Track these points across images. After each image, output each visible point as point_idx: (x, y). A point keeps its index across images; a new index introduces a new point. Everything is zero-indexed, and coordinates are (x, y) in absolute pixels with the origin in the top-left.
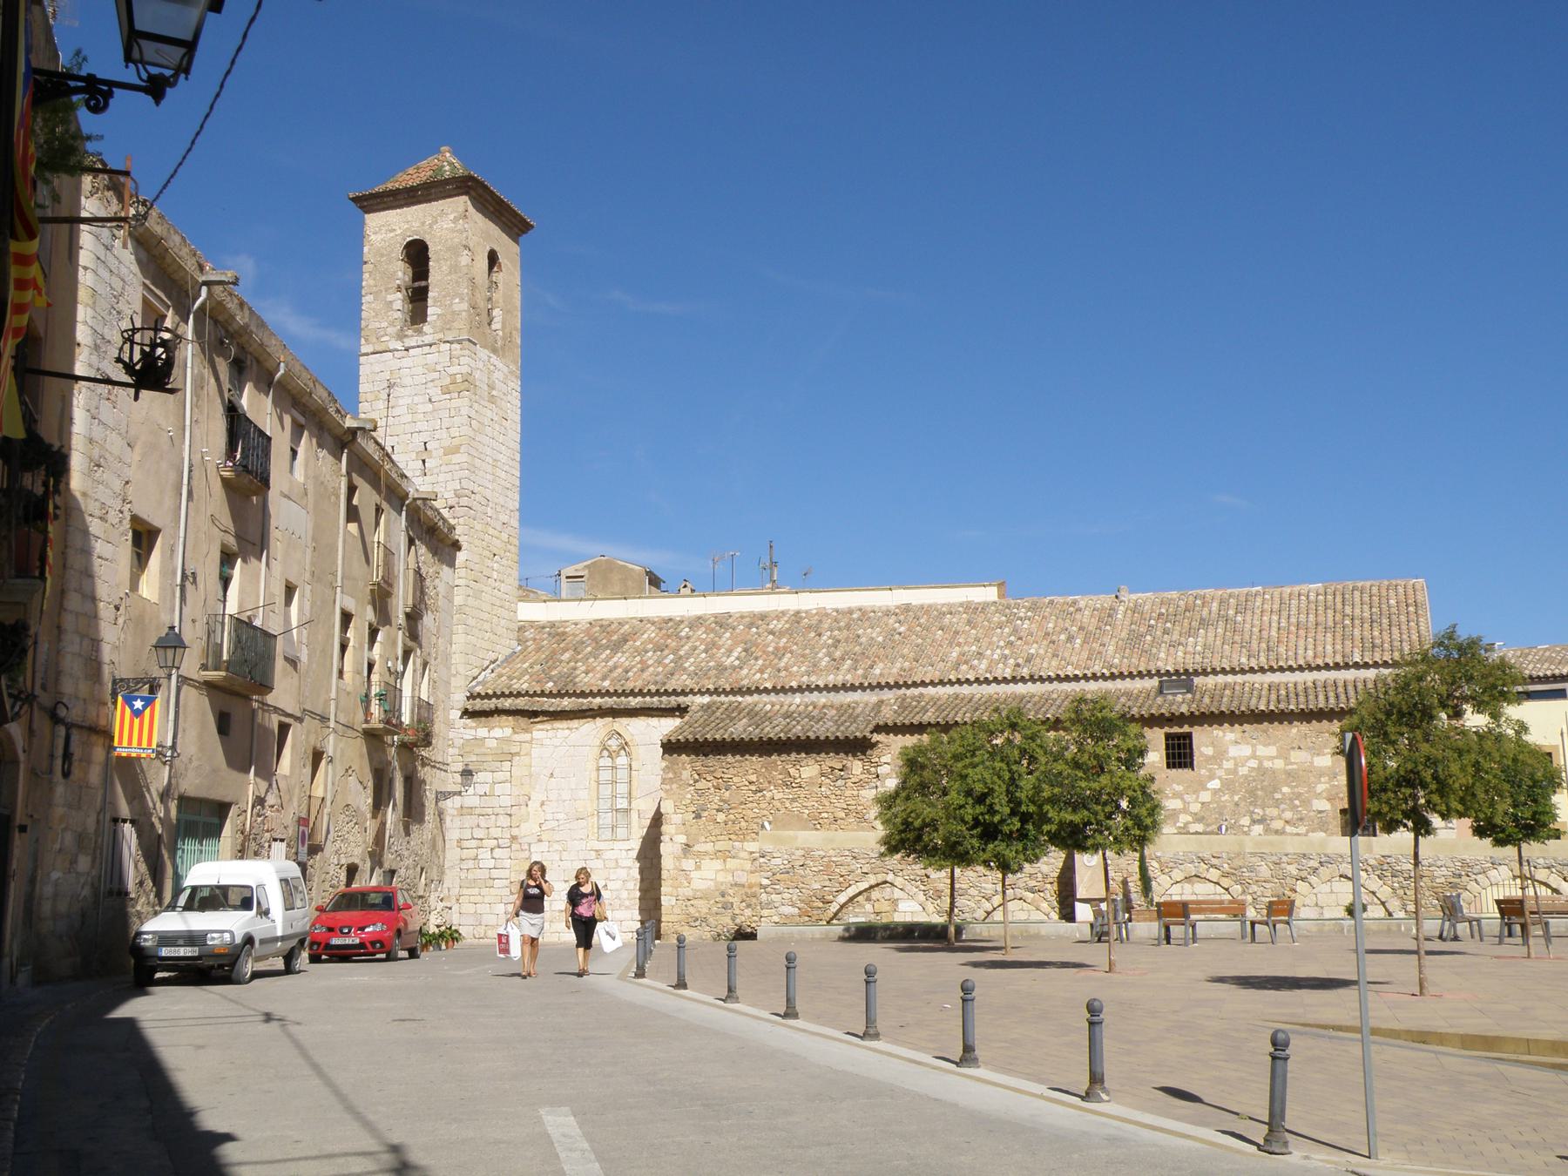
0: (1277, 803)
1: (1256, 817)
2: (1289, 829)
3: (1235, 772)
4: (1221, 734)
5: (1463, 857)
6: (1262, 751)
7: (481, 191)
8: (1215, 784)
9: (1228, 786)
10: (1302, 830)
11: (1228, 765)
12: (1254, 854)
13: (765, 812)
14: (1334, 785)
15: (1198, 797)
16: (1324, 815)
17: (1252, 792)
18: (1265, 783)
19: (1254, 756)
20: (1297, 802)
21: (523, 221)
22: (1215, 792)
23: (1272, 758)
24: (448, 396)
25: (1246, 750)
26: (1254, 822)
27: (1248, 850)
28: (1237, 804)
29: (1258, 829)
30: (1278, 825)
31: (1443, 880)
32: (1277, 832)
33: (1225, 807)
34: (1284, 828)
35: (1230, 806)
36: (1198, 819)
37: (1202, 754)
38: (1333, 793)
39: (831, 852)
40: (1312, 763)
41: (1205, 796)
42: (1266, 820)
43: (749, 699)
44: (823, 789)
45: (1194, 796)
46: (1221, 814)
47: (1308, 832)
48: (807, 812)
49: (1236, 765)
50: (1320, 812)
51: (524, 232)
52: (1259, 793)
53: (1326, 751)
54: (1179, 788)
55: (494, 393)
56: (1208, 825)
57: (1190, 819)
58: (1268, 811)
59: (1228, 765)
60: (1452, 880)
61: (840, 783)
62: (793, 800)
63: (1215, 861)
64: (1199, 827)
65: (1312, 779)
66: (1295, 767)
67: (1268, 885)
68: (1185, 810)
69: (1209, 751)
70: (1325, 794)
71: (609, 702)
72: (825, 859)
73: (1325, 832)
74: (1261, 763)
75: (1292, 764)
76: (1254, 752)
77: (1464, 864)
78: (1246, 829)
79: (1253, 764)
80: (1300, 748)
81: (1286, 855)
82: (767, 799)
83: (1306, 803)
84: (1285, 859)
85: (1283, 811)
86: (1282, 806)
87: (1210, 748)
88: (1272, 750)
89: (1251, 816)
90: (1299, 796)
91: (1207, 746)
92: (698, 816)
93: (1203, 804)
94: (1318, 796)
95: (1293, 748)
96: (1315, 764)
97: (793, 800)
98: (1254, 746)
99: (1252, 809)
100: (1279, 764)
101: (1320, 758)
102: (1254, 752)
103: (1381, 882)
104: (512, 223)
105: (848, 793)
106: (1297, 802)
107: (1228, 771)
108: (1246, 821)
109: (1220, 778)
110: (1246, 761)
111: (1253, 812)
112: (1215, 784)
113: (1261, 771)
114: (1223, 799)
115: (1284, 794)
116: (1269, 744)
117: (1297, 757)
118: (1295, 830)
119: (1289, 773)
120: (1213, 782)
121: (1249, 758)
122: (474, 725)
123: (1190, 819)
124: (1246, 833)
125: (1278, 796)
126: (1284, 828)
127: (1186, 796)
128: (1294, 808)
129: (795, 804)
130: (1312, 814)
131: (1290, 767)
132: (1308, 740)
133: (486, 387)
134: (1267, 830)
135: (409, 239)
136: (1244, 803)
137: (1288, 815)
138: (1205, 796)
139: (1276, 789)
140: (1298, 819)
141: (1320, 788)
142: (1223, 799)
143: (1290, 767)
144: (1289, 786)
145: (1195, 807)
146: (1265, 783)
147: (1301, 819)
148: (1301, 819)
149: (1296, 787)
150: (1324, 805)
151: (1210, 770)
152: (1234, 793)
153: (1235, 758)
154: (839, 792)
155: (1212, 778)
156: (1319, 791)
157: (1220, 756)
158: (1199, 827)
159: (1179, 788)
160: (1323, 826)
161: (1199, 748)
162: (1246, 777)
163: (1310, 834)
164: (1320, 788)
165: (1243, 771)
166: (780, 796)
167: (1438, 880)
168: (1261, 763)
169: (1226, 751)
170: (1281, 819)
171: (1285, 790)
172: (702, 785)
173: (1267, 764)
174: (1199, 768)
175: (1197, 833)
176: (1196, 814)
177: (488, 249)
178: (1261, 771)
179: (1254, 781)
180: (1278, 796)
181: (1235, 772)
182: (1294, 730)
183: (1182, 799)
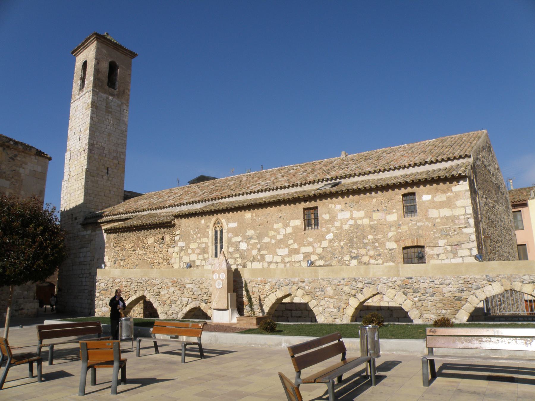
0: (365, 246)
1: (353, 255)
2: (372, 261)
3: (341, 228)
4: (333, 206)
5: (465, 277)
6: (357, 214)
7: (103, 39)
8: (330, 236)
9: (337, 237)
10: (380, 261)
11: (338, 224)
12: (324, 280)
13: (136, 261)
14: (399, 232)
15: (321, 244)
16: (393, 251)
17: (351, 240)
18: (358, 234)
19: (352, 218)
20: (377, 244)
21: (131, 52)
22: (331, 241)
23: (361, 218)
24: (86, 111)
25: (346, 215)
26: (352, 258)
27: (320, 277)
28: (342, 248)
29: (354, 262)
30: (365, 259)
31: (450, 294)
32: (365, 263)
33: (336, 249)
34: (369, 261)
35: (339, 248)
36: (321, 257)
37: (323, 219)
38: (398, 237)
39: (123, 280)
40: (385, 219)
41: (325, 244)
42: (358, 256)
43: (163, 211)
44: (155, 249)
45: (319, 244)
46: (333, 254)
47: (383, 263)
48: (149, 260)
49: (342, 224)
50: (391, 250)
51: (134, 57)
52: (355, 240)
53: (394, 211)
54: (311, 240)
55: (110, 110)
56: (326, 261)
57: (316, 258)
58: (360, 250)
59: (338, 224)
60: (457, 294)
61: (161, 245)
62: (145, 255)
63: (301, 284)
64: (321, 262)
65: (385, 230)
66: (375, 222)
67: (332, 300)
68: (314, 253)
69: (327, 217)
70: (393, 239)
71: (123, 216)
72: (121, 283)
73: (394, 262)
74: (356, 222)
75: (373, 220)
76: (352, 215)
77: (466, 282)
78: (347, 262)
79: (351, 222)
80: (378, 211)
81: (344, 279)
82: (137, 254)
83: (383, 244)
84: (342, 282)
85: (369, 251)
86: (368, 248)
87: (328, 215)
88: (362, 213)
89: (350, 255)
90: (377, 240)
91: (326, 214)
92: (115, 263)
93: (323, 248)
94: (389, 240)
95: (374, 211)
96: (387, 220)
97: (145, 255)
98: (351, 212)
99: (351, 250)
100: (366, 221)
101: (390, 215)
102: (352, 215)
103: (405, 297)
104: (126, 53)
105: (164, 250)
106: (377, 244)
107: (338, 228)
108: (347, 258)
109: (333, 232)
110: (348, 221)
111: (351, 252)
112: (330, 236)
113: (356, 227)
114: (335, 245)
115: (369, 240)
116: (360, 210)
117: (376, 216)
118: (376, 262)
119: (372, 227)
120: (329, 235)
121: (349, 219)
122: (83, 230)
123: (316, 258)
124: (347, 265)
125: (366, 241)
126: (369, 261)
127: (314, 244)
128: (375, 248)
129: (146, 256)
130: (386, 251)
131: (373, 223)
132: (383, 205)
133: (105, 108)
134: (360, 263)
135: (84, 61)
136: (346, 247)
137: (372, 253)
138: (325, 244)
139: (364, 237)
140: (377, 255)
141: (390, 234)
142: (335, 245)
143: (373, 223)
144: (372, 235)
145: (319, 251)
146: (358, 234)
147: (380, 255)
148: (380, 255)
149: (376, 235)
150: (392, 245)
151: (327, 228)
152: (340, 241)
153: (341, 220)
154: (161, 250)
155: (328, 232)
156: (389, 237)
157: (333, 219)
158: (321, 262)
159: (311, 240)
160: (392, 259)
161: (321, 216)
162: (347, 231)
163: (385, 264)
164: (390, 234)
165: (346, 227)
166: (140, 253)
167: (446, 295)
168: (356, 222)
169: (336, 216)
170: (367, 255)
171: (370, 237)
172: (117, 249)
173: (359, 222)
174: (322, 227)
175: (320, 266)
176: (320, 255)
177: (110, 60)
178: (356, 227)
179: (352, 233)
180: (366, 241)
181: (341, 228)
182: (375, 200)
183: (313, 246)
